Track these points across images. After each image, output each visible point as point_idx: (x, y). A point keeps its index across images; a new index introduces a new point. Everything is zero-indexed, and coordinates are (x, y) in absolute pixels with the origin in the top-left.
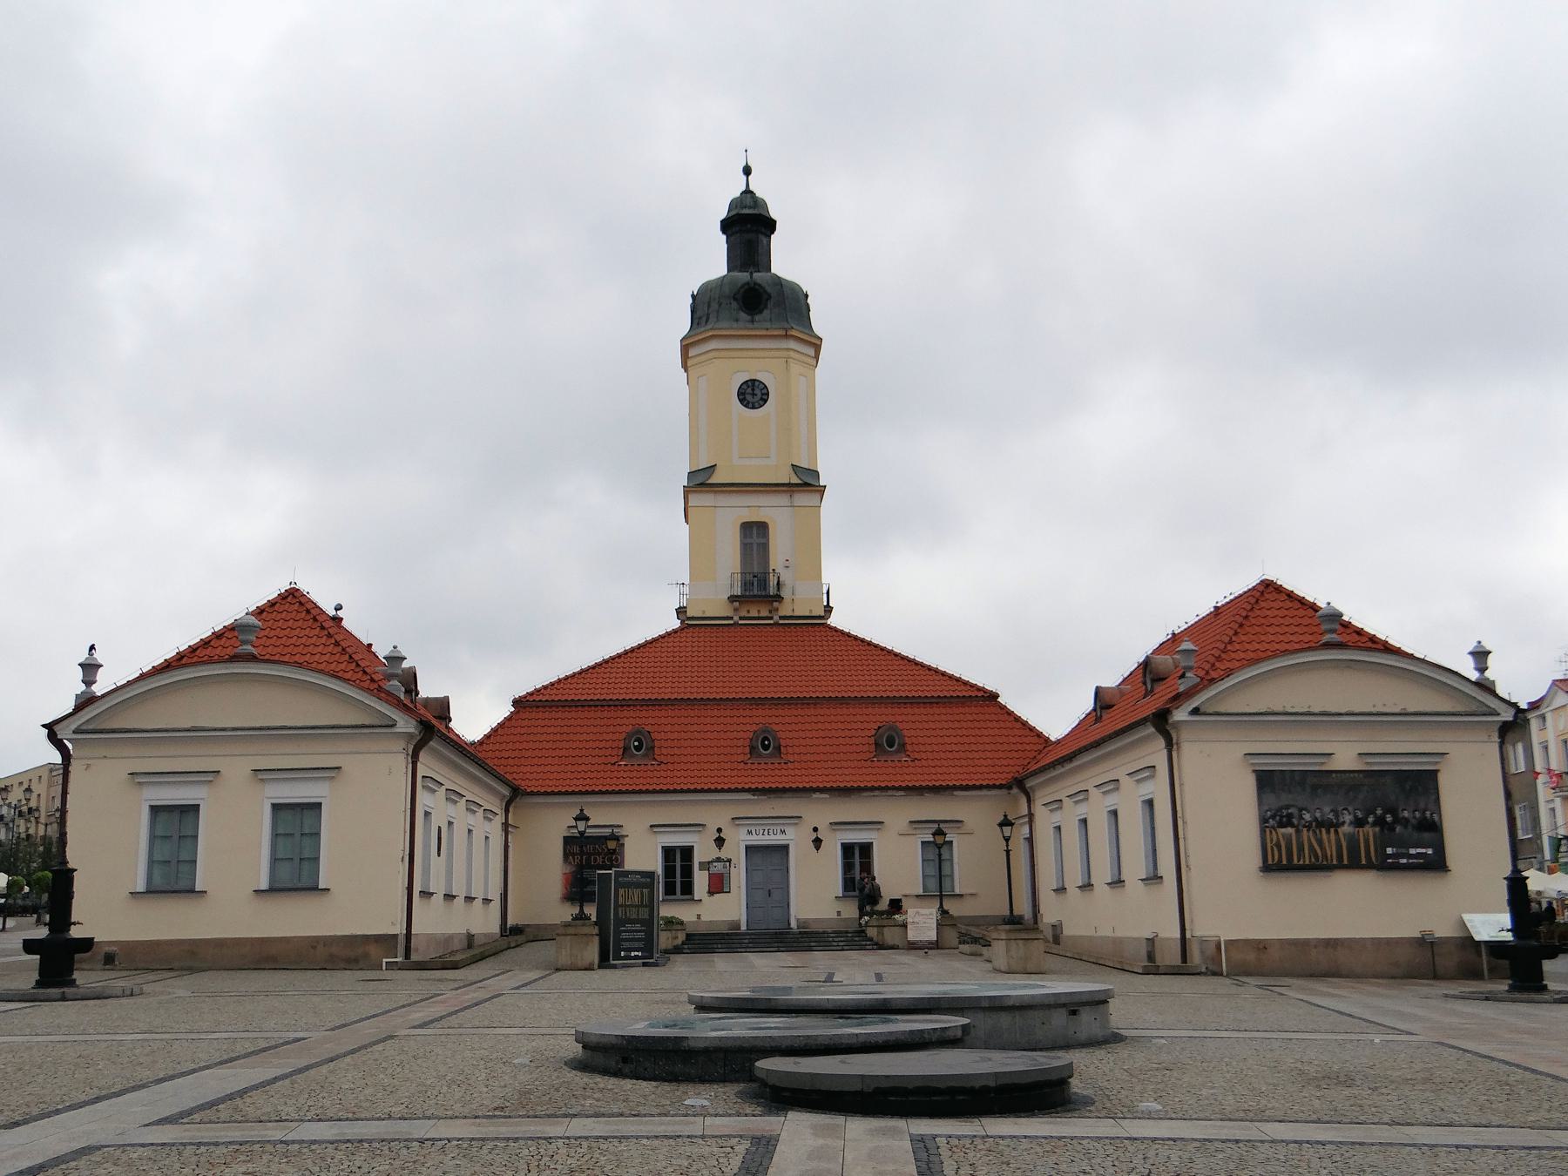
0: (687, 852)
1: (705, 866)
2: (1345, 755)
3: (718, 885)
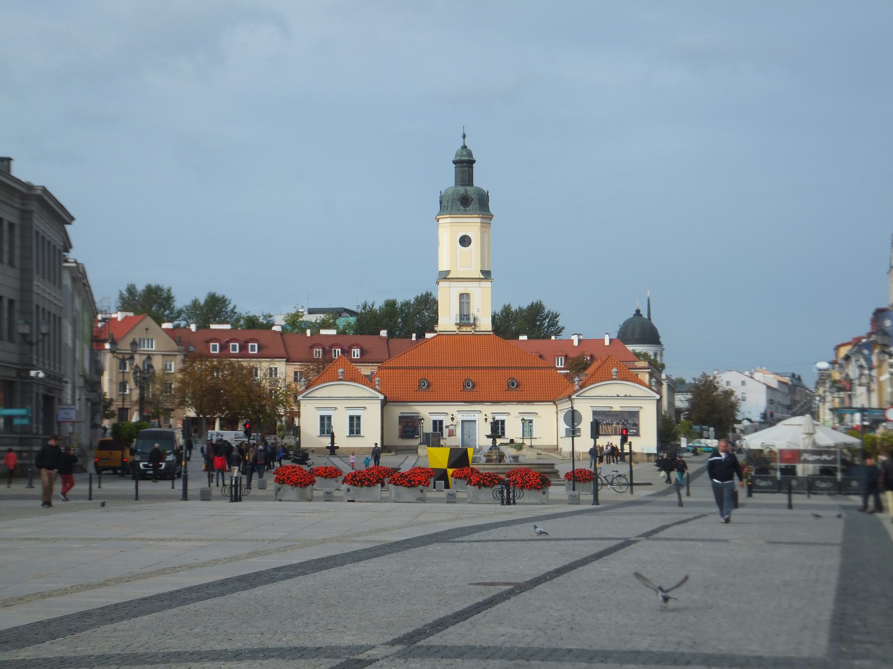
0: (441, 422)
1: (447, 427)
2: (617, 406)
3: (452, 434)
